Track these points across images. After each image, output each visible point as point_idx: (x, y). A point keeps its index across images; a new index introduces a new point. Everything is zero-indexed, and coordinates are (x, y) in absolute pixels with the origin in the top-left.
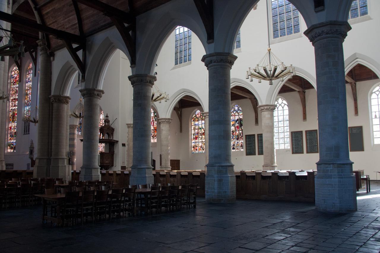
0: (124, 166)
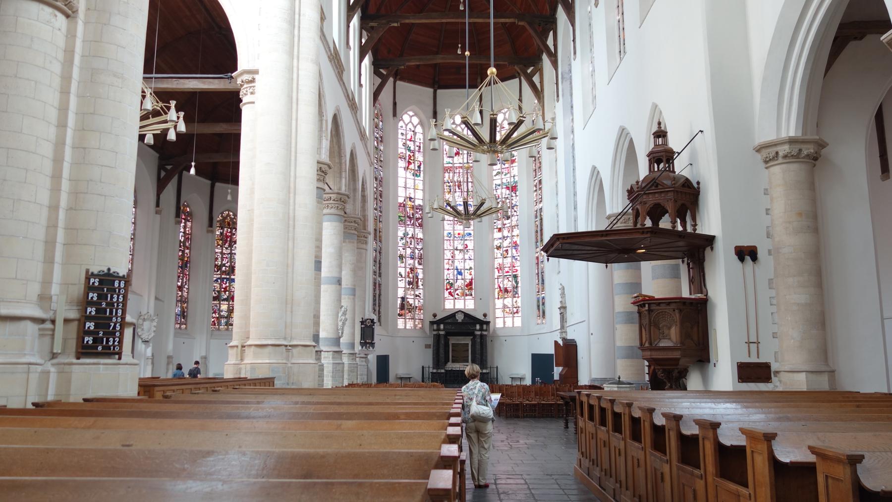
0: (754, 359)
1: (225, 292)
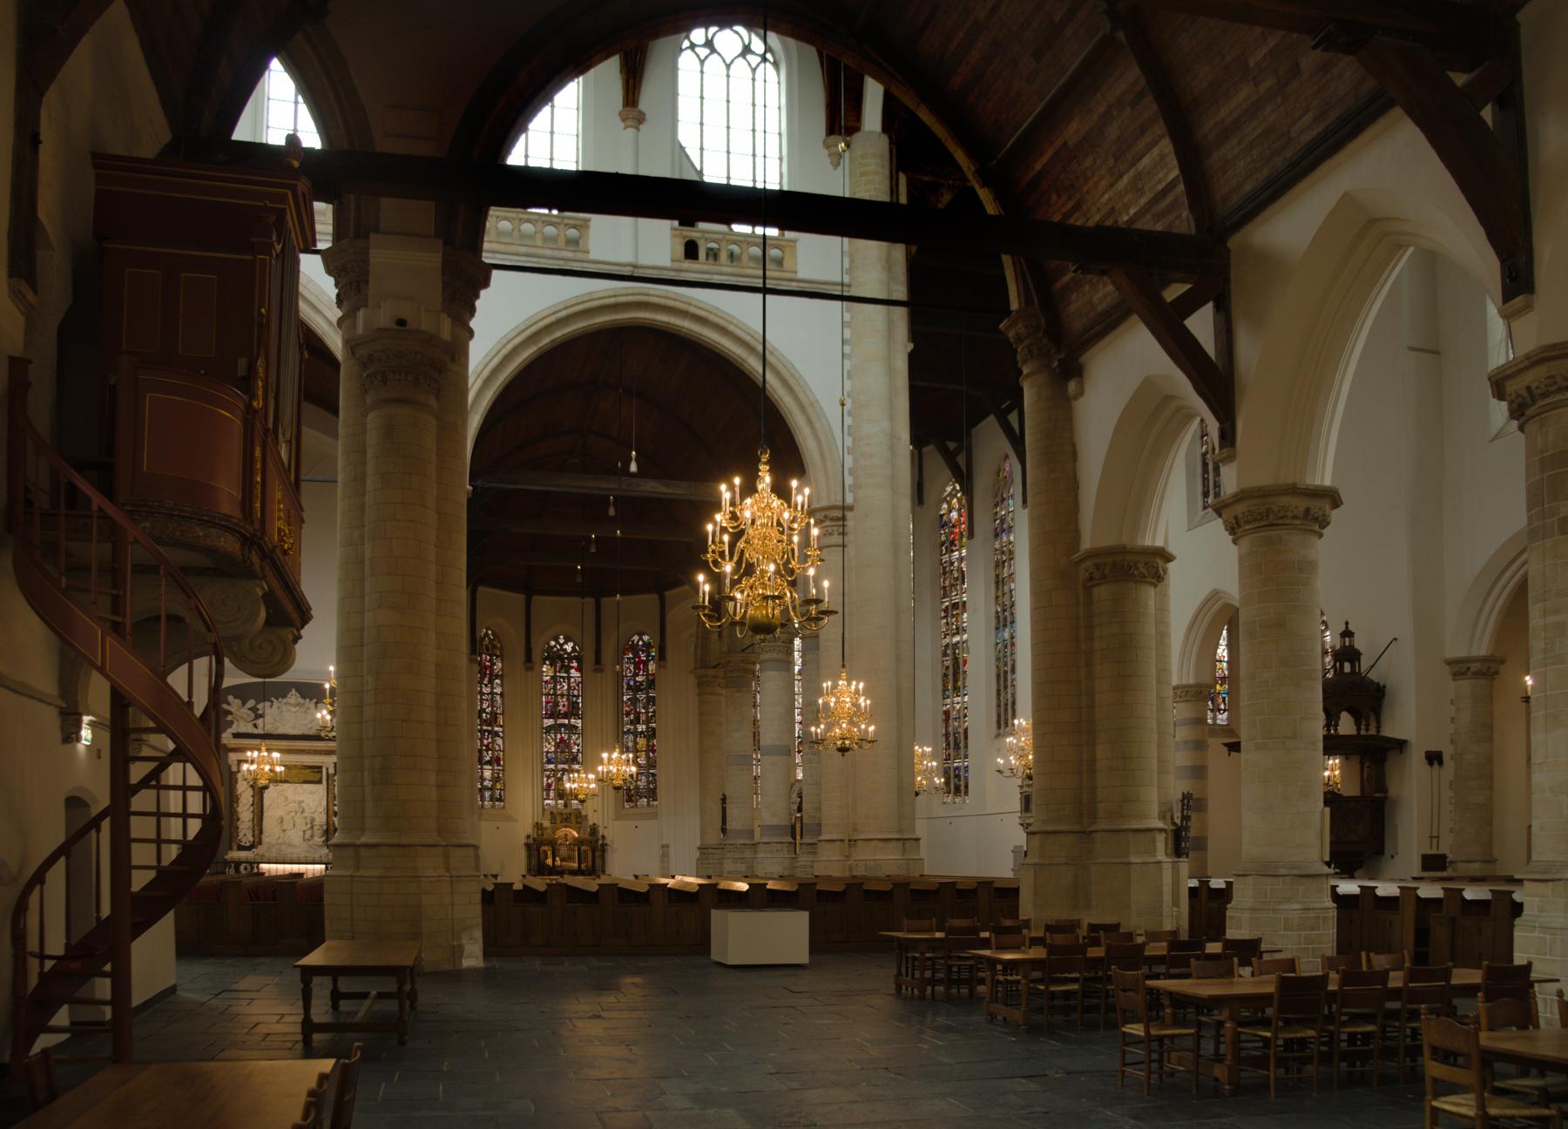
0: (1434, 852)
1: (487, 751)
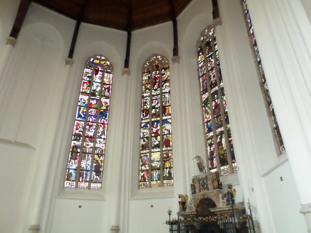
1: (156, 137)
